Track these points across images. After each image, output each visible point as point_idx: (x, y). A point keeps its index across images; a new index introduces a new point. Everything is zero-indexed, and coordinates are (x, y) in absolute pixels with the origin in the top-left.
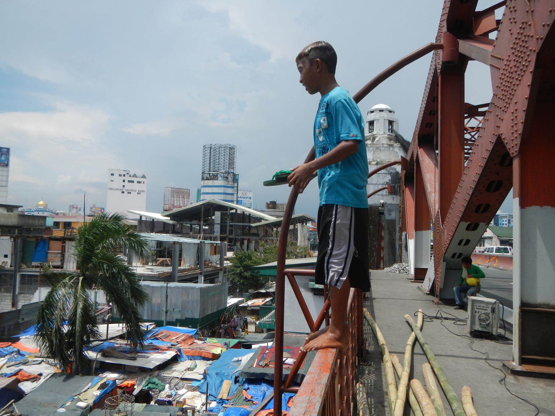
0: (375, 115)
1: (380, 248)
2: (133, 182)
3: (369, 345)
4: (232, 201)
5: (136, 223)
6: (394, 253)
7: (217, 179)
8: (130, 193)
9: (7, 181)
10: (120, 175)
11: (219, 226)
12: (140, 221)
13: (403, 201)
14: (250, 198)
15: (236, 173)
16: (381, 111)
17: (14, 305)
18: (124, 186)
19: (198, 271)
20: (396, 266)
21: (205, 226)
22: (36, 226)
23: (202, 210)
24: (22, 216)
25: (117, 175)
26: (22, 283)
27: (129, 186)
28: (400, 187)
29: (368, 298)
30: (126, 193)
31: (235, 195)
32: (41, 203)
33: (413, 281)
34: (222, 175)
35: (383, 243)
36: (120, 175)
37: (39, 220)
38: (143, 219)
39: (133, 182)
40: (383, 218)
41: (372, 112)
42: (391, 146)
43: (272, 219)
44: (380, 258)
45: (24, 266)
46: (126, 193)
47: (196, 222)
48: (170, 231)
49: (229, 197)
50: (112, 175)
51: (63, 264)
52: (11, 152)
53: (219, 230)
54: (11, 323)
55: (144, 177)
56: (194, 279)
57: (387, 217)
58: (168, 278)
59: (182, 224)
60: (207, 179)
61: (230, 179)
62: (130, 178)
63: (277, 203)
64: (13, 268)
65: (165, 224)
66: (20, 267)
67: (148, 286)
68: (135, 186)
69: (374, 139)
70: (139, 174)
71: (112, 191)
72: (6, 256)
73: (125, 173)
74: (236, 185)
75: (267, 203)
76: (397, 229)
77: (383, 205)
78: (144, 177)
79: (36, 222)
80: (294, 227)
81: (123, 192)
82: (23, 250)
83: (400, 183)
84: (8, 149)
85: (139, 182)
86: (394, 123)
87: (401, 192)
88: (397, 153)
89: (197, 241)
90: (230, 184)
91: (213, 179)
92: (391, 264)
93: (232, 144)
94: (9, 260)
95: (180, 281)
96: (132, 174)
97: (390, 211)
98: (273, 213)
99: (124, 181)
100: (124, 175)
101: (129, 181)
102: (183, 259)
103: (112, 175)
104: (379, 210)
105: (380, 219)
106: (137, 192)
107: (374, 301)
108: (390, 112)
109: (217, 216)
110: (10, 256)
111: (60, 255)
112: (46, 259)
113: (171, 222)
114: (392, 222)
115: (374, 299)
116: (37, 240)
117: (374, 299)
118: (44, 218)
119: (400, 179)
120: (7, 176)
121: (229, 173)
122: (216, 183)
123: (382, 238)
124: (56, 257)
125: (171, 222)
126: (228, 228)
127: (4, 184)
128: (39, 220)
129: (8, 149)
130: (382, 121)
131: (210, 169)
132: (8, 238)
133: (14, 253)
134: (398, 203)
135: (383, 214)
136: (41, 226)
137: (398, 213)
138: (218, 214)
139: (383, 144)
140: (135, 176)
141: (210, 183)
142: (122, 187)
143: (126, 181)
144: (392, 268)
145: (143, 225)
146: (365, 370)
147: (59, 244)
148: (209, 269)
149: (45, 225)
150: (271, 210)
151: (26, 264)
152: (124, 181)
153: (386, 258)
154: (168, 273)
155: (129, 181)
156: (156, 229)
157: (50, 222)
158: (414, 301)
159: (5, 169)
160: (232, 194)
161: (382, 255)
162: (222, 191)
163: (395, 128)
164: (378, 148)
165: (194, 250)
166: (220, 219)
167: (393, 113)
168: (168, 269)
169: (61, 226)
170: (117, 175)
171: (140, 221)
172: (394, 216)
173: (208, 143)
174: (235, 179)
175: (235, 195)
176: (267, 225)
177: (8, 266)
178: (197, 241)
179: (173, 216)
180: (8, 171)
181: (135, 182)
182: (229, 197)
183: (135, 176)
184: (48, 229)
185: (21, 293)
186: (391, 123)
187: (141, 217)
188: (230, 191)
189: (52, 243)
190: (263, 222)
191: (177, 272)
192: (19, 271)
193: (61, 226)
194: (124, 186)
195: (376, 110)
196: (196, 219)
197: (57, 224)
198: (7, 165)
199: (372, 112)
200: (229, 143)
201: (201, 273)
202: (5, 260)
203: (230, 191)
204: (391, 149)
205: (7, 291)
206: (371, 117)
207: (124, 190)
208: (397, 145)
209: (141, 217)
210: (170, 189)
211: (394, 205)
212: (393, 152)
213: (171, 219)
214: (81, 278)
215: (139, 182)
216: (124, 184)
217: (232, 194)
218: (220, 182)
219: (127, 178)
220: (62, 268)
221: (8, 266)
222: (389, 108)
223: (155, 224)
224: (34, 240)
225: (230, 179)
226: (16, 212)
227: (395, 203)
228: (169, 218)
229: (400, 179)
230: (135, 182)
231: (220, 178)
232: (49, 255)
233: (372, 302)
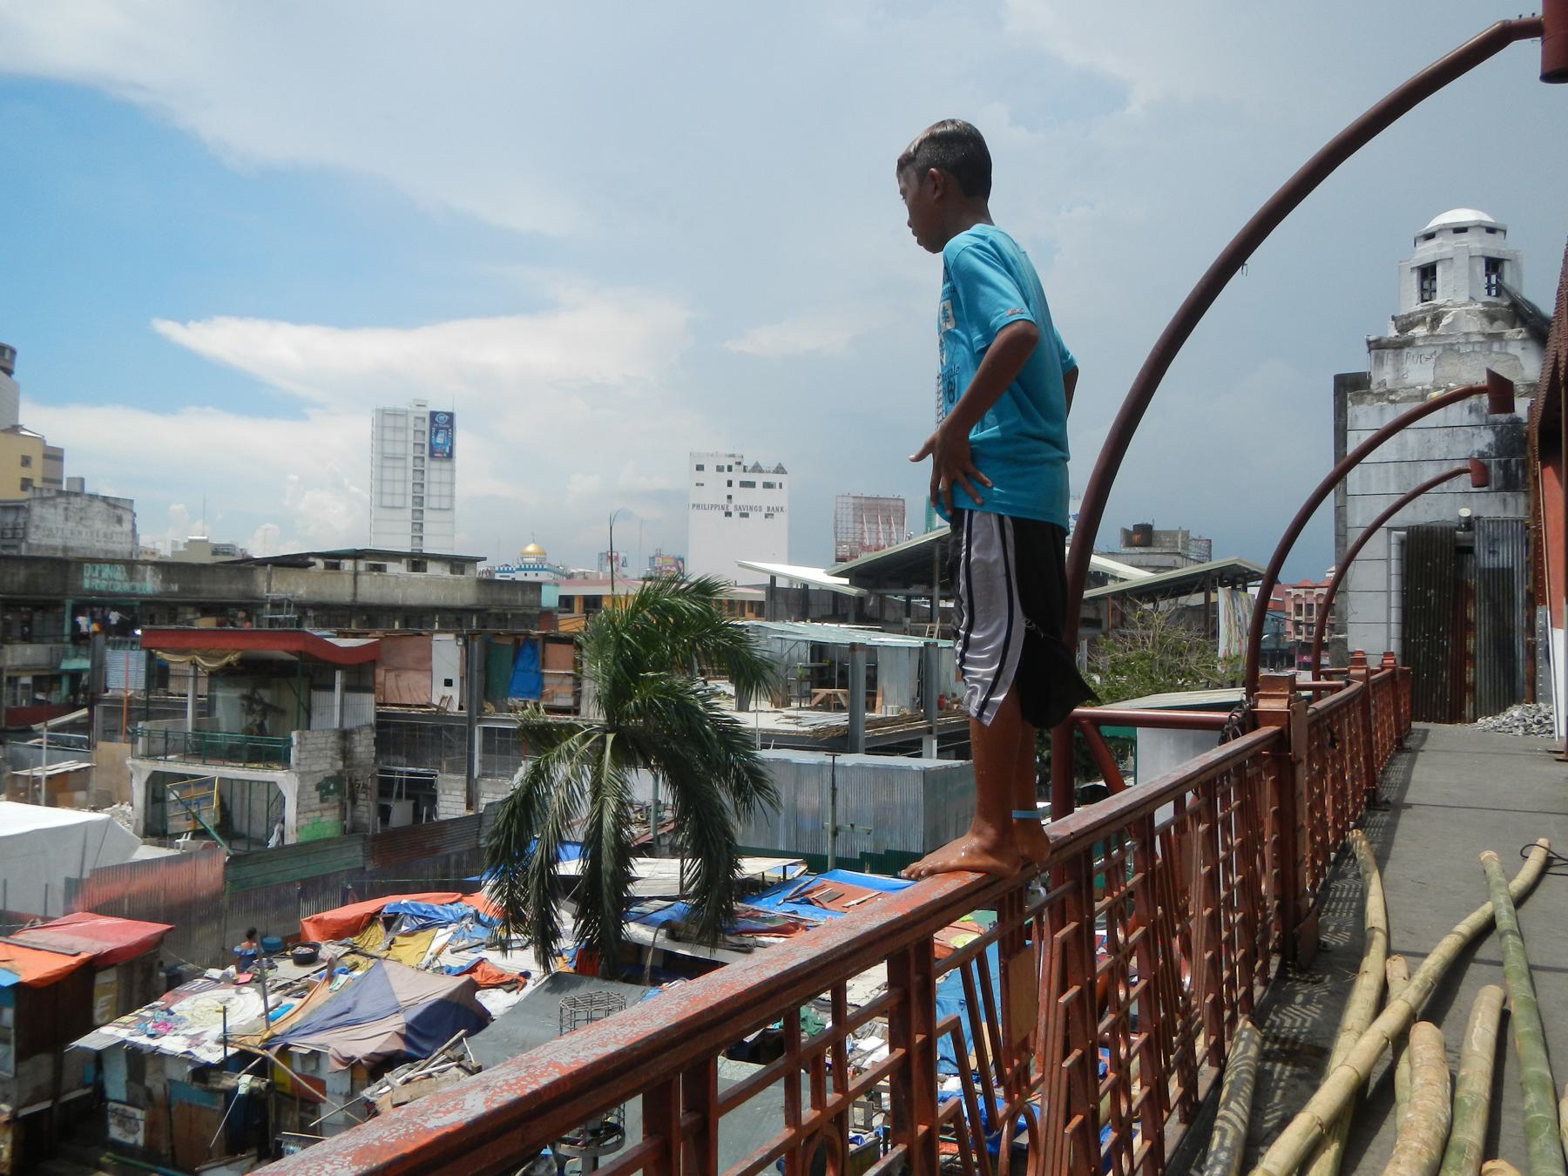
0: (1441, 245)
1: (1463, 658)
2: (752, 485)
3: (1337, 931)
5: (760, 595)
6: (1511, 673)
8: (746, 515)
9: (452, 496)
10: (720, 469)
12: (772, 589)
13: (1535, 510)
16: (1460, 230)
17: (469, 805)
18: (730, 497)
19: (921, 725)
20: (1516, 712)
21: (947, 599)
22: (517, 607)
23: (937, 554)
24: (487, 583)
25: (710, 468)
26: (487, 749)
27: (742, 497)
28: (1524, 465)
29: (1387, 802)
30: (736, 514)
32: (531, 548)
33: (1561, 757)
35: (1471, 643)
36: (720, 469)
37: (524, 592)
38: (781, 583)
39: (752, 485)
40: (1470, 563)
41: (1430, 236)
42: (1498, 337)
43: (1140, 576)
44: (1461, 689)
45: (490, 707)
46: (736, 514)
47: (920, 589)
48: (852, 615)
50: (700, 468)
51: (578, 703)
52: (458, 422)
54: (464, 846)
55: (780, 470)
56: (911, 747)
57: (1485, 559)
58: (839, 742)
59: (882, 597)
62: (745, 474)
63: (1155, 528)
64: (464, 712)
65: (836, 596)
66: (481, 709)
67: (786, 762)
68: (758, 497)
69: (1437, 320)
70: (768, 463)
71: (701, 512)
72: (448, 683)
73: (732, 462)
75: (1126, 532)
76: (1520, 596)
77: (1469, 524)
78: (780, 470)
79: (519, 598)
80: (1207, 598)
81: (728, 514)
82: (486, 669)
83: (1524, 452)
84: (451, 416)
85: (768, 485)
86: (1507, 265)
87: (1530, 479)
88: (1516, 358)
89: (917, 642)
92: (1500, 706)
94: (454, 693)
95: (869, 751)
96: (749, 463)
97: (1493, 541)
98: (1144, 560)
99: (730, 484)
100: (730, 468)
101: (743, 484)
102: (879, 692)
103: (700, 468)
104: (1456, 540)
105: (1460, 567)
106: (765, 511)
107: (1405, 813)
108: (1491, 230)
110: (456, 682)
111: (570, 681)
112: (537, 690)
113: (854, 591)
114: (1503, 577)
115: (1409, 806)
116: (517, 641)
117: (1409, 806)
118: (537, 586)
119: (1525, 441)
120: (452, 484)
123: (1469, 626)
124: (560, 684)
125: (854, 591)
127: (445, 504)
128: (524, 592)
129: (451, 416)
130: (1462, 262)
132: (451, 637)
133: (467, 677)
134: (1521, 514)
135: (1470, 550)
136: (531, 607)
137: (1521, 548)
139: (1467, 334)
140: (757, 469)
142: (724, 501)
143: (736, 484)
144: (1503, 718)
145: (780, 599)
146: (1295, 994)
148: (953, 720)
149: (539, 605)
150: (1137, 549)
151: (494, 703)
152: (730, 484)
153: (1483, 688)
154: (838, 728)
155: (743, 484)
156: (814, 612)
157: (549, 598)
158: (1541, 817)
159: (446, 465)
161: (1469, 678)
163: (1508, 279)
164: (1450, 349)
165: (909, 668)
167: (1499, 235)
168: (839, 719)
169: (578, 606)
170: (710, 468)
171: (772, 589)
172: (1508, 556)
176: (1121, 596)
177: (454, 708)
178: (917, 642)
180: (453, 470)
181: (759, 485)
183: (757, 469)
184: (547, 615)
185: (484, 775)
186: (1493, 265)
187: (773, 579)
189: (550, 647)
190: (1112, 587)
191: (861, 726)
192: (480, 721)
193: (578, 606)
194: (730, 497)
195: (1443, 229)
196: (920, 582)
197: (566, 602)
198: (450, 456)
199: (1430, 236)
201: (930, 731)
202: (448, 691)
204: (1496, 347)
205: (454, 769)
206: (1426, 253)
207: (731, 509)
208: (1515, 334)
209: (773, 579)
210: (851, 500)
211: (1505, 521)
212: (1503, 358)
213: (852, 584)
214: (610, 737)
215: (768, 485)
216: (729, 491)
219: (738, 476)
220: (577, 712)
221: (454, 708)
222: (1487, 218)
223: (812, 598)
224: (509, 641)
226: (472, 574)
227: (1511, 514)
228: (846, 581)
229: (1525, 441)
230: (759, 485)
232: (547, 680)
233: (1397, 815)
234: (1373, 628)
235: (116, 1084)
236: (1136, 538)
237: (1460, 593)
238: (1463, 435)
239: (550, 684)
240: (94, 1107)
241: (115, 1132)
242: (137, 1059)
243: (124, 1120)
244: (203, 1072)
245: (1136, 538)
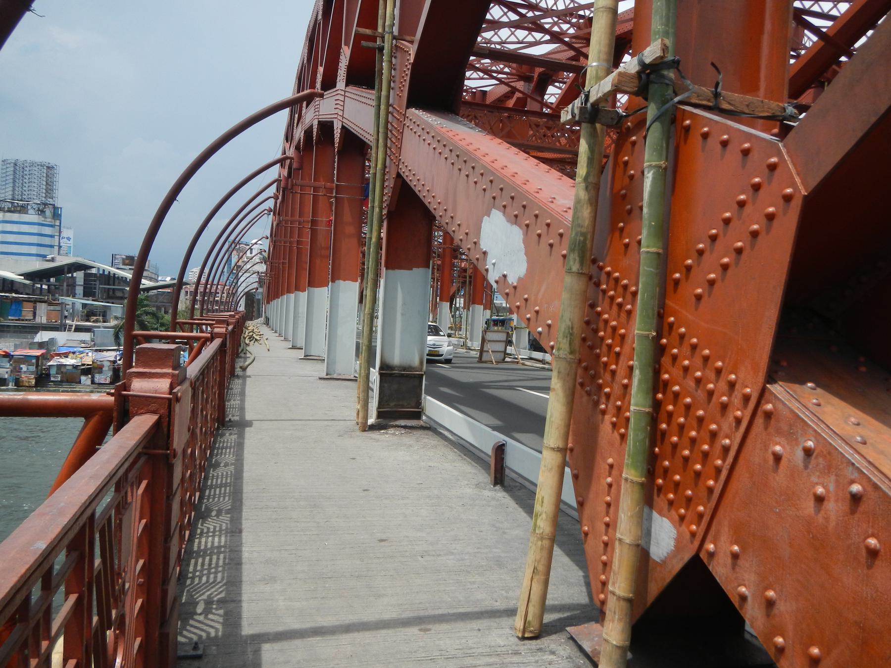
1: (253, 312)
4: (52, 246)
7: (27, 213)
11: (82, 288)
14: (69, 239)
15: (58, 205)
31: (57, 238)
34: (35, 206)
49: (47, 241)
53: (82, 292)
60: (9, 211)
61: (48, 212)
74: (57, 223)
90: (49, 221)
91: (19, 212)
93: (52, 163)
109: (79, 276)
112: (20, 315)
113: (27, 282)
121: (45, 204)
122: (25, 218)
126: (97, 291)
131: (13, 195)
138: (79, 276)
141: (15, 217)
147: (31, 304)
160: (52, 236)
162: (36, 231)
166: (83, 280)
172: (260, 297)
173: (12, 157)
174: (56, 215)
175: (57, 238)
179: (27, 276)
182: (47, 241)
188: (47, 231)
189: (25, 303)
200: (48, 161)
203: (47, 231)
217: (52, 236)
218: (32, 217)
225: (48, 212)
231: (31, 211)
234: (242, 308)
235: (53, 371)
236: (127, 261)
237: (253, 302)
238: (255, 278)
239: (23, 313)
240: (48, 375)
241: (52, 379)
242: (60, 367)
243: (55, 377)
244: (75, 367)
245: (127, 261)
